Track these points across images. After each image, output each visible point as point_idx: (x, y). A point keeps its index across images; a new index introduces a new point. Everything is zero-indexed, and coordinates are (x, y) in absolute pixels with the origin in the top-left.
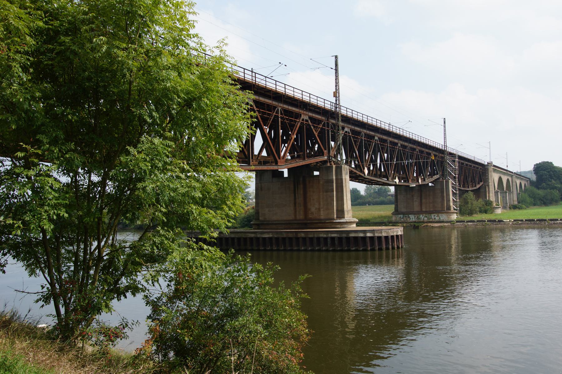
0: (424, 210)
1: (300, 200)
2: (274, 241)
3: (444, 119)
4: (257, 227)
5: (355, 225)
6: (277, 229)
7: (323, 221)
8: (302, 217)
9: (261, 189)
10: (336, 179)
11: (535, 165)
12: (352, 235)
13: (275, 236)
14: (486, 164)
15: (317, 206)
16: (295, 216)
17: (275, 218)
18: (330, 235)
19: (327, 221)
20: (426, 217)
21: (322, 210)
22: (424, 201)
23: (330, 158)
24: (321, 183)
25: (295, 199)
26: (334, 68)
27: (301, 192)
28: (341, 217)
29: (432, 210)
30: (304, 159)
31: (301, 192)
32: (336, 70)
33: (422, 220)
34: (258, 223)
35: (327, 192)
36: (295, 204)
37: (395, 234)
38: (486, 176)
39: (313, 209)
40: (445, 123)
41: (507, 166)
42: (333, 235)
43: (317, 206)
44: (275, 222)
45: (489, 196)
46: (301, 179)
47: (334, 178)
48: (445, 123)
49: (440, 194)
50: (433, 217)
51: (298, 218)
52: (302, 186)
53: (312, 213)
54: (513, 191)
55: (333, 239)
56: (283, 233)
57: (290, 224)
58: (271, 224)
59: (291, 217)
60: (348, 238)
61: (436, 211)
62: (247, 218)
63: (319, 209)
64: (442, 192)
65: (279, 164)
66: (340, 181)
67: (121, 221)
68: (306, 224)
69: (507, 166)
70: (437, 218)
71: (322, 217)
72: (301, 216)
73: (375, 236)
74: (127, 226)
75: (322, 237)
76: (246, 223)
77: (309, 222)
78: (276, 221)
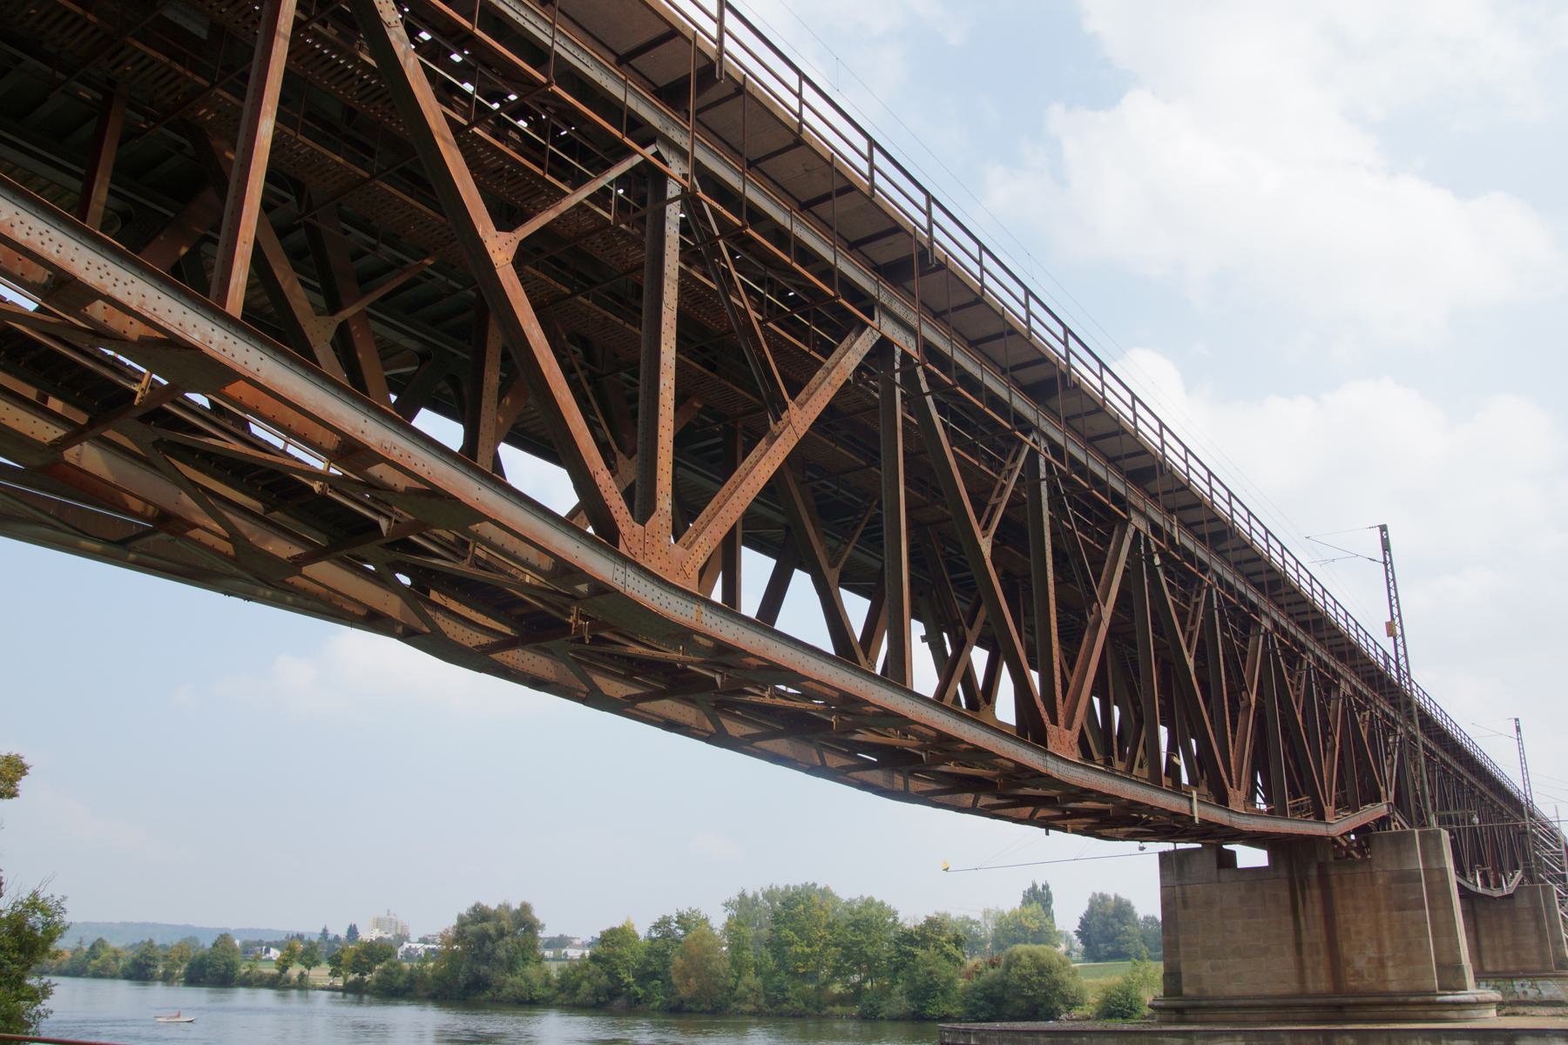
0: (1489, 968)
1: (1314, 933)
4: (1174, 1017)
5: (1493, 1012)
6: (1245, 1022)
7: (1400, 999)
9: (1185, 904)
15: (1371, 952)
17: (1233, 989)
19: (1413, 999)
21: (1390, 964)
22: (1485, 942)
26: (1378, 554)
28: (1454, 985)
29: (1512, 967)
31: (1315, 909)
32: (1387, 564)
34: (1178, 1003)
35: (1401, 909)
36: (1298, 946)
39: (1360, 963)
40: (1518, 729)
43: (1371, 952)
44: (1235, 1003)
46: (1313, 872)
47: (1421, 867)
48: (1518, 729)
49: (1532, 924)
50: (1518, 989)
51: (1311, 987)
52: (1316, 893)
53: (1358, 974)
56: (1282, 1035)
57: (1286, 1007)
58: (1222, 1007)
59: (1289, 986)
61: (1525, 971)
62: (983, 990)
63: (1381, 963)
64: (1538, 918)
65: (1328, 820)
67: (624, 989)
68: (1340, 1007)
70: (1532, 993)
72: (1319, 983)
74: (638, 1001)
76: (981, 1003)
77: (1351, 1001)
78: (1238, 998)
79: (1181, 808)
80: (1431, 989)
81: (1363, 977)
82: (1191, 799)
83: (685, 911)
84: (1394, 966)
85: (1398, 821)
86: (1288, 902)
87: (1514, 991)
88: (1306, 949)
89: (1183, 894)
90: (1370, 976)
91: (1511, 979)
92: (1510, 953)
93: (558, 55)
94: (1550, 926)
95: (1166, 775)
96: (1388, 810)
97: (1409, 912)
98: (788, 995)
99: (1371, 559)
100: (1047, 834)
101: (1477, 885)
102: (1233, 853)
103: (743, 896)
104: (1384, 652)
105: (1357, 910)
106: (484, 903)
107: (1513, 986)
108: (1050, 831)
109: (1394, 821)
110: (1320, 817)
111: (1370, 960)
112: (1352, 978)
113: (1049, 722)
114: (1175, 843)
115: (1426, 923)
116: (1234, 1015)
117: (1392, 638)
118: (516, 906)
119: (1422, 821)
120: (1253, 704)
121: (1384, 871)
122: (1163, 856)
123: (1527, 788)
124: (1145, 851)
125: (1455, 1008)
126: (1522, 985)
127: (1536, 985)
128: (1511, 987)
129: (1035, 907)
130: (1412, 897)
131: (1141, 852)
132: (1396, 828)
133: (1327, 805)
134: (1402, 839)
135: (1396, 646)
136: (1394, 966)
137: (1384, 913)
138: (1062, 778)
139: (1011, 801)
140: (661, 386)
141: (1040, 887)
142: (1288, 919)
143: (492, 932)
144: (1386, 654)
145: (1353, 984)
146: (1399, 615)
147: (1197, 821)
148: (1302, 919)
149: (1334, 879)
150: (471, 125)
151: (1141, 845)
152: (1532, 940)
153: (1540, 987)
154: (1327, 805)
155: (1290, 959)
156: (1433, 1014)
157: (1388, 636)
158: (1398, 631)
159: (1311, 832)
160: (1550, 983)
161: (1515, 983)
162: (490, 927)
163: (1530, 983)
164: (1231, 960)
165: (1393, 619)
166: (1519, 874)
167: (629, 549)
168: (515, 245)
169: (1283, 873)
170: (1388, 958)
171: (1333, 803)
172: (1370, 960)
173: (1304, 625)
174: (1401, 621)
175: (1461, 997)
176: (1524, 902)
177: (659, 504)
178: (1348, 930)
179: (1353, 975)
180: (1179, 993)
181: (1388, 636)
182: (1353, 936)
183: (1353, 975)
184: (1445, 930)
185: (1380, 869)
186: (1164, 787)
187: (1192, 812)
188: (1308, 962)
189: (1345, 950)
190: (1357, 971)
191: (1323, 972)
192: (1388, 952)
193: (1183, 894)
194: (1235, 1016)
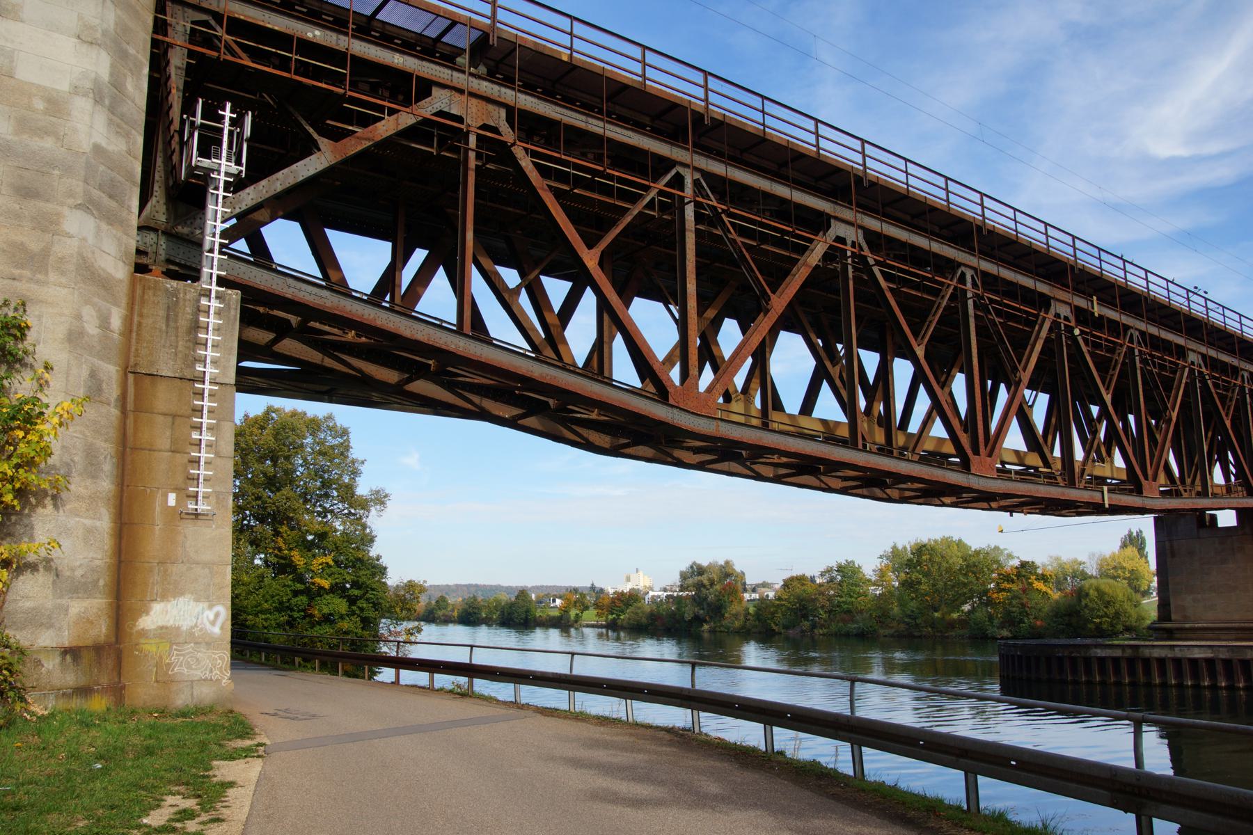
2: (1219, 667)
83: (843, 562)
93: (610, 140)
98: (918, 621)
100: (1011, 515)
102: (1214, 518)
103: (894, 548)
106: (698, 562)
108: (1014, 514)
118: (722, 562)
129: (1131, 551)
140: (688, 307)
141: (1135, 534)
143: (706, 582)
147: (1107, 506)
150: (572, 190)
162: (704, 579)
167: (674, 400)
168: (599, 253)
173: (1231, 351)
177: (691, 373)
180: (1169, 619)
187: (1104, 501)
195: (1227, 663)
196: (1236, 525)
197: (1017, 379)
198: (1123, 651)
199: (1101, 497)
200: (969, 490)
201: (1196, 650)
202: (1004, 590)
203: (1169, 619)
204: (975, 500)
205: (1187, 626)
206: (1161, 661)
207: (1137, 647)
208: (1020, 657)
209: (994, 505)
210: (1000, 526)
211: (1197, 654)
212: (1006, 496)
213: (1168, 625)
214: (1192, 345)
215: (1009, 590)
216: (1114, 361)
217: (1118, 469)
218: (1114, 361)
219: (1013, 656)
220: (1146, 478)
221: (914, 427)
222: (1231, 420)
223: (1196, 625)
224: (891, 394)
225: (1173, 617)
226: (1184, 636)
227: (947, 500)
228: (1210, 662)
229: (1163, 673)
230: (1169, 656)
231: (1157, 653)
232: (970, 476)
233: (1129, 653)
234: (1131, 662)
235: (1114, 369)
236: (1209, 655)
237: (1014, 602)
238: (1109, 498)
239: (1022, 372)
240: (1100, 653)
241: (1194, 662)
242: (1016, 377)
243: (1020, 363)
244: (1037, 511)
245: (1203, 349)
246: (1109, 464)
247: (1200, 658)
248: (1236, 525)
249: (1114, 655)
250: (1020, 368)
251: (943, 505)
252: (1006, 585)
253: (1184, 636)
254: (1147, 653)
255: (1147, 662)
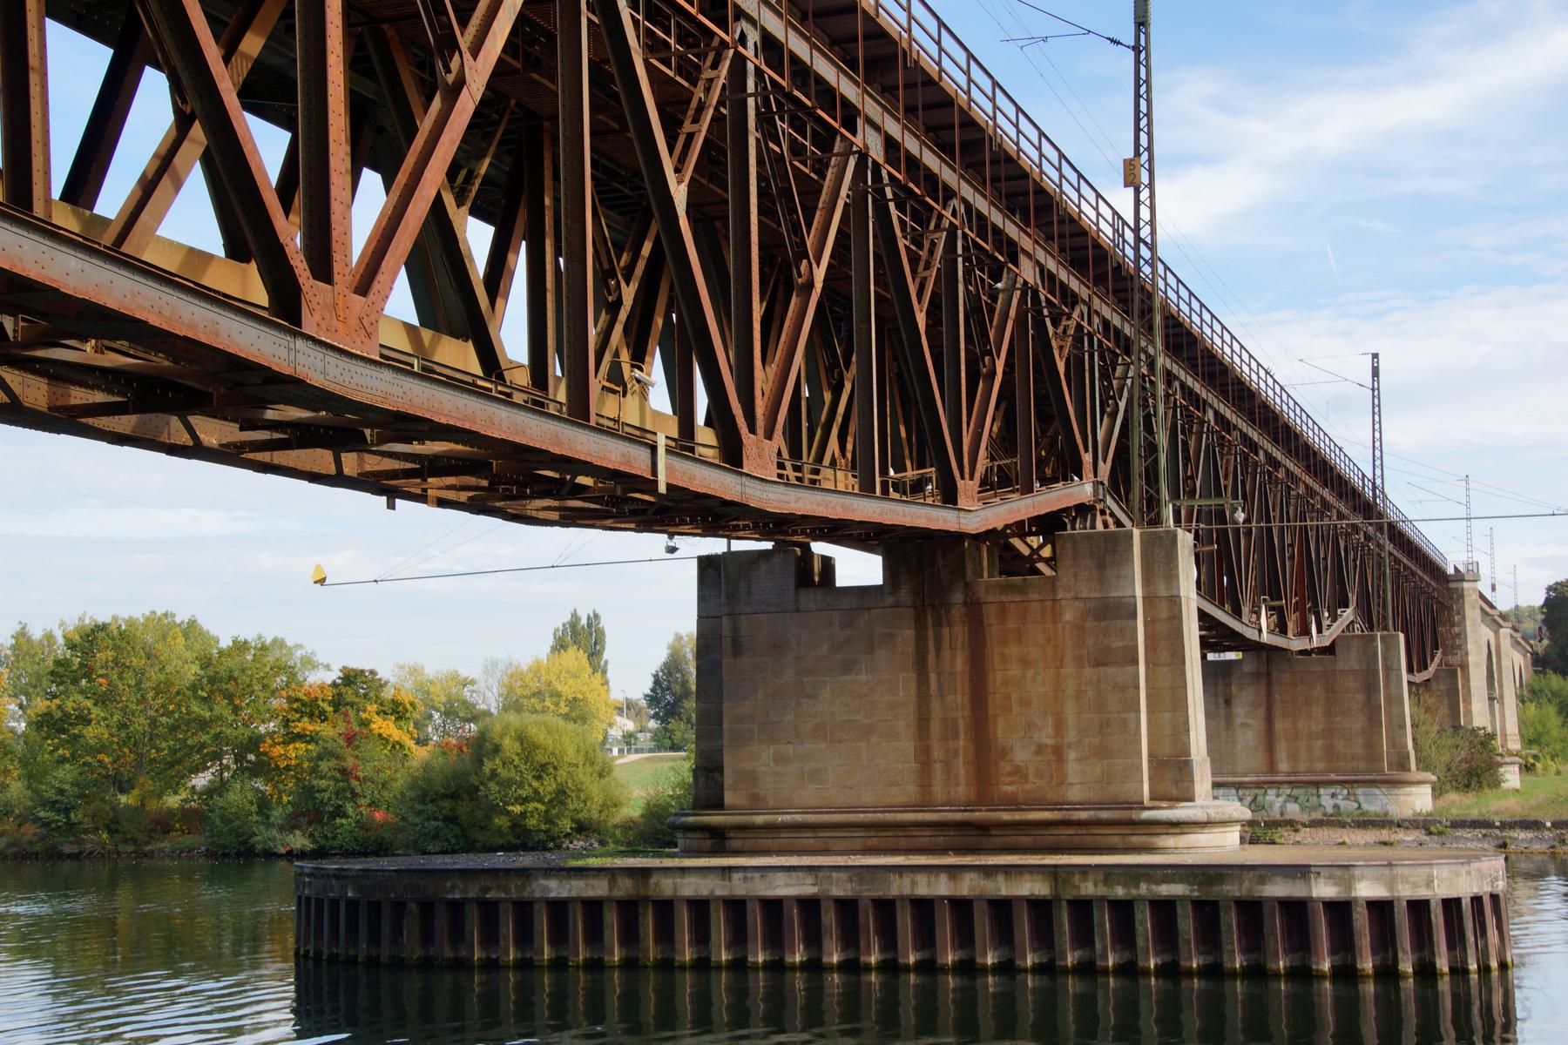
2: (829, 918)
3: (1375, 356)
4: (708, 843)
5: (1232, 837)
7: (1084, 815)
8: (962, 791)
10: (1147, 599)
11: (1549, 589)
12: (1278, 889)
13: (837, 892)
14: (1451, 571)
15: (1046, 736)
16: (924, 780)
18: (1143, 889)
20: (1296, 799)
21: (1072, 756)
22: (1280, 726)
23: (1101, 491)
24: (1068, 616)
25: (923, 698)
27: (960, 663)
30: (1028, 489)
32: (1140, 50)
33: (1275, 814)
35: (1099, 664)
36: (923, 721)
37: (1487, 889)
38: (1453, 625)
39: (1022, 755)
40: (1375, 372)
41: (1493, 589)
42: (1166, 890)
45: (1469, 712)
47: (1139, 592)
48: (1375, 372)
49: (1360, 697)
52: (958, 632)
54: (1502, 696)
55: (1164, 909)
60: (1251, 910)
63: (1059, 752)
64: (1370, 687)
65: (962, 503)
66: (1163, 612)
68: (983, 828)
69: (1493, 589)
71: (1074, 794)
73: (1399, 899)
75: (1102, 899)
77: (1006, 817)
79: (628, 463)
80: (1139, 799)
81: (1026, 777)
82: (654, 449)
84: (1079, 760)
85: (1112, 514)
86: (911, 648)
87: (1320, 805)
88: (935, 726)
89: (735, 630)
90: (1039, 775)
91: (1317, 784)
92: (1318, 744)
94: (1388, 699)
95: (708, 423)
96: (1096, 492)
97: (1110, 670)
99: (1112, 41)
100: (391, 506)
101: (1260, 631)
102: (828, 563)
104: (1115, 213)
105: (1025, 662)
107: (1319, 796)
108: (398, 501)
109: (1103, 512)
110: (949, 497)
111: (1040, 749)
112: (1008, 779)
113: (308, 273)
114: (729, 538)
115: (1137, 687)
116: (808, 840)
117: (1131, 191)
119: (1150, 514)
120: (819, 285)
121: (1076, 598)
122: (707, 565)
123: (1378, 472)
124: (676, 555)
125: (1170, 831)
126: (1333, 795)
127: (1355, 794)
128: (1315, 798)
129: (575, 658)
130: (1120, 644)
131: (670, 556)
132: (1106, 525)
133: (962, 478)
134: (1115, 545)
135: (1137, 202)
136: (1079, 760)
137: (1069, 670)
138: (331, 387)
139: (277, 436)
141: (584, 621)
142: (908, 678)
144: (1120, 217)
145: (1006, 788)
146: (1149, 149)
147: (662, 489)
148: (933, 677)
149: (990, 614)
151: (671, 544)
152: (1357, 723)
153: (1361, 799)
154: (962, 478)
155: (908, 745)
156: (1135, 839)
157: (1126, 186)
158: (1145, 178)
159: (921, 523)
160: (1377, 791)
161: (1322, 791)
163: (1345, 792)
164: (808, 746)
165: (1137, 154)
166: (1348, 614)
169: (905, 595)
170: (1069, 746)
171: (977, 476)
172: (1040, 749)
174: (1151, 160)
175: (1181, 812)
176: (1349, 661)
178: (1008, 697)
179: (1011, 774)
180: (718, 804)
181: (1126, 186)
182: (1015, 709)
183: (1011, 774)
184: (1171, 701)
185: (1069, 595)
186: (592, 423)
187: (654, 472)
188: (937, 753)
189: (1001, 730)
190: (1018, 767)
191: (961, 768)
192: (1071, 735)
193: (735, 630)
194: (812, 841)
195: (847, 907)
196: (880, 582)
197: (450, 78)
198: (613, 883)
199: (648, 462)
200: (292, 388)
201: (780, 878)
202: (300, 737)
203: (718, 804)
204: (302, 436)
205: (759, 819)
206: (700, 907)
207: (645, 873)
208: (353, 904)
209: (351, 463)
210: (318, 566)
211: (783, 887)
212: (405, 425)
213: (716, 819)
214: (872, 109)
215: (312, 739)
216: (694, 104)
217: (656, 414)
218: (694, 104)
219: (334, 903)
220: (752, 430)
221: (112, 200)
222: (927, 313)
223: (780, 818)
224: (33, 61)
225: (729, 798)
226: (749, 844)
227: (213, 431)
228: (809, 906)
229: (702, 935)
230: (719, 893)
231: (691, 887)
232: (300, 344)
233: (625, 888)
234: (629, 908)
235: (696, 120)
236: (807, 888)
237: (324, 766)
238: (669, 468)
239: (467, 56)
240: (556, 889)
241: (773, 907)
242: (448, 71)
243: (464, 24)
244: (463, 496)
245: (894, 129)
246: (636, 398)
247: (787, 898)
248: (880, 582)
249: (590, 893)
250: (464, 42)
251: (196, 450)
252: (306, 725)
253: (749, 844)
254: (666, 887)
255: (665, 908)
